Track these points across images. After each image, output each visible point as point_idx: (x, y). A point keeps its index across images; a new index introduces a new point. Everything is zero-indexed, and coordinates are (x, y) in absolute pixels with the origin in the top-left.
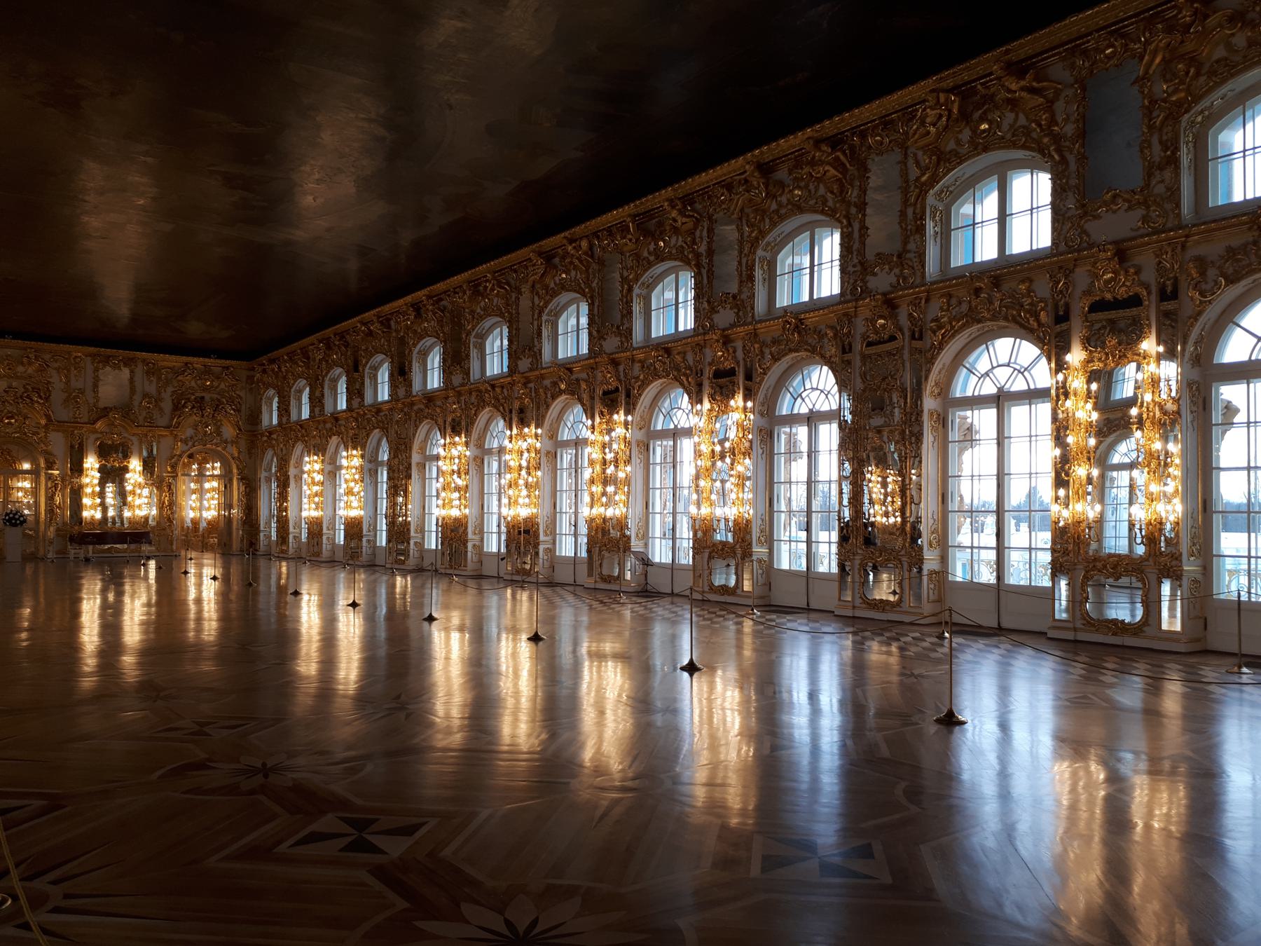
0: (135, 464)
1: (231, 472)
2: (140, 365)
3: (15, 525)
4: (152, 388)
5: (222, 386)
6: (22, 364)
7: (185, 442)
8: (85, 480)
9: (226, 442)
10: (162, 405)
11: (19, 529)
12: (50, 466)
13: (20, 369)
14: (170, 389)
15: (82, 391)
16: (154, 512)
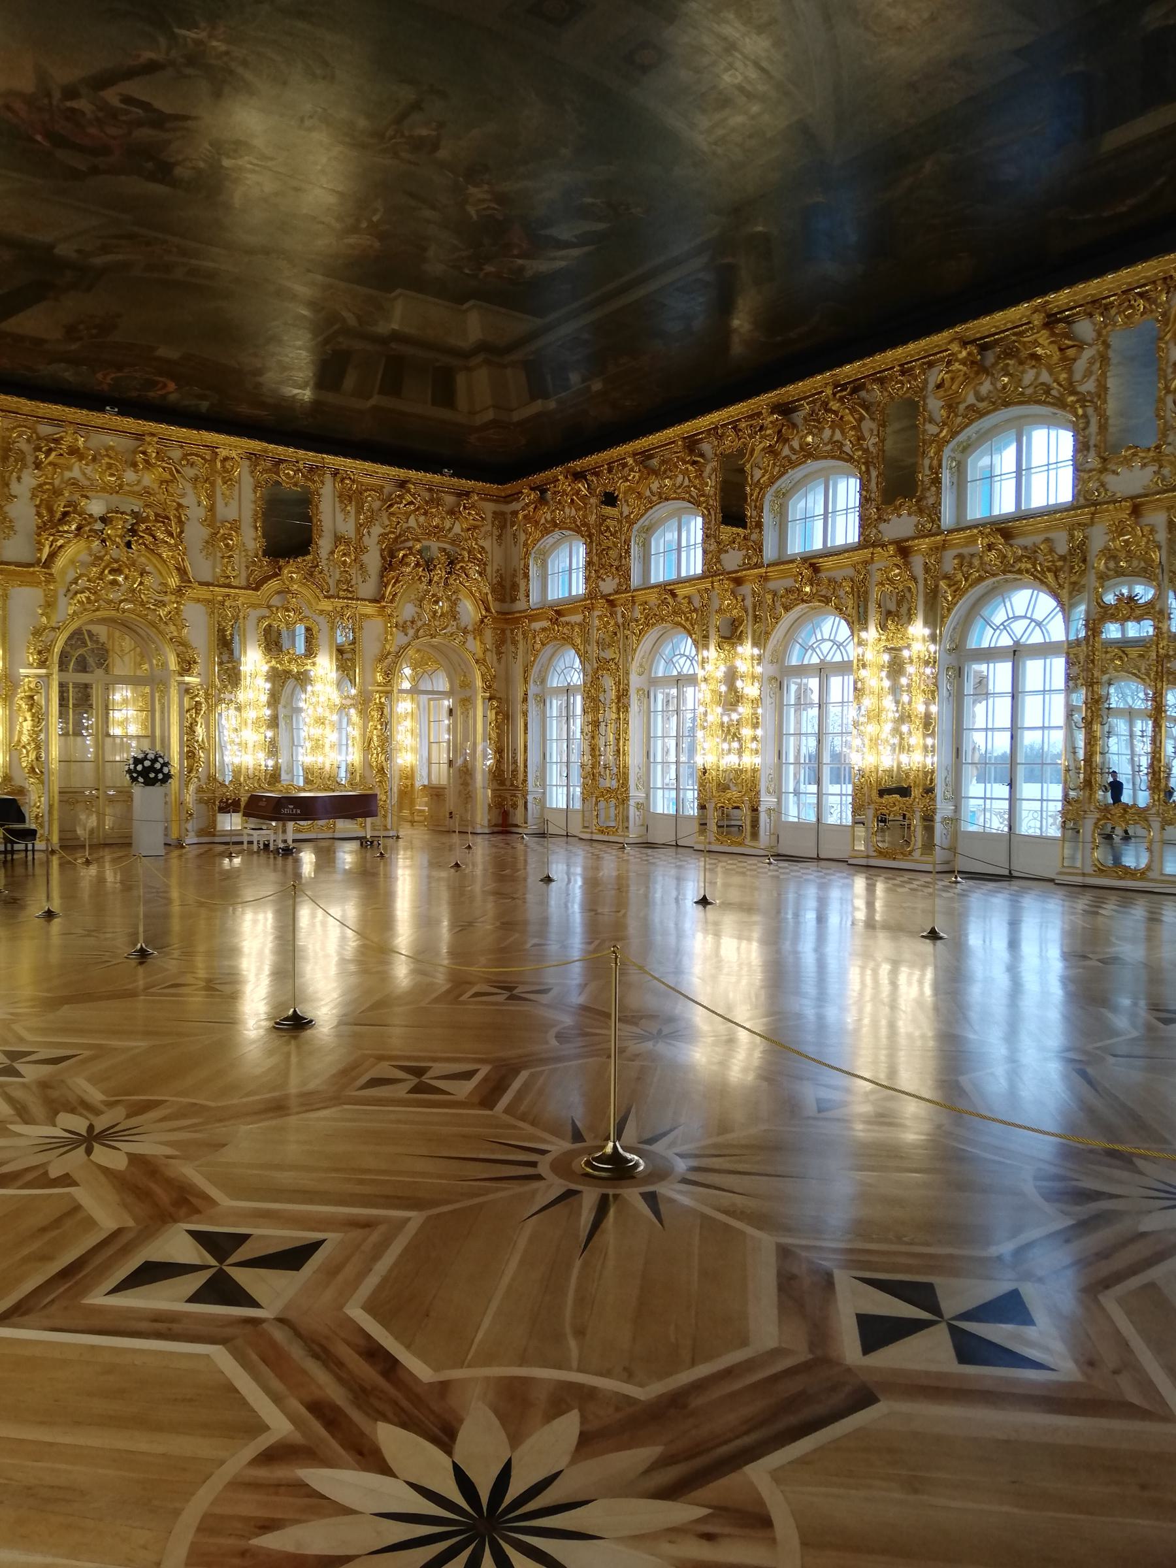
0: (324, 667)
1: (466, 685)
2: (328, 477)
3: (149, 782)
4: (348, 528)
5: (457, 529)
6: (134, 465)
7: (403, 627)
8: (242, 696)
9: (465, 631)
10: (365, 558)
11: (157, 790)
12: (187, 666)
13: (130, 476)
14: (377, 530)
15: (235, 526)
16: (355, 756)
